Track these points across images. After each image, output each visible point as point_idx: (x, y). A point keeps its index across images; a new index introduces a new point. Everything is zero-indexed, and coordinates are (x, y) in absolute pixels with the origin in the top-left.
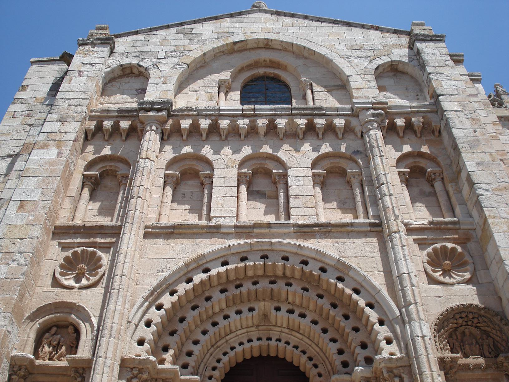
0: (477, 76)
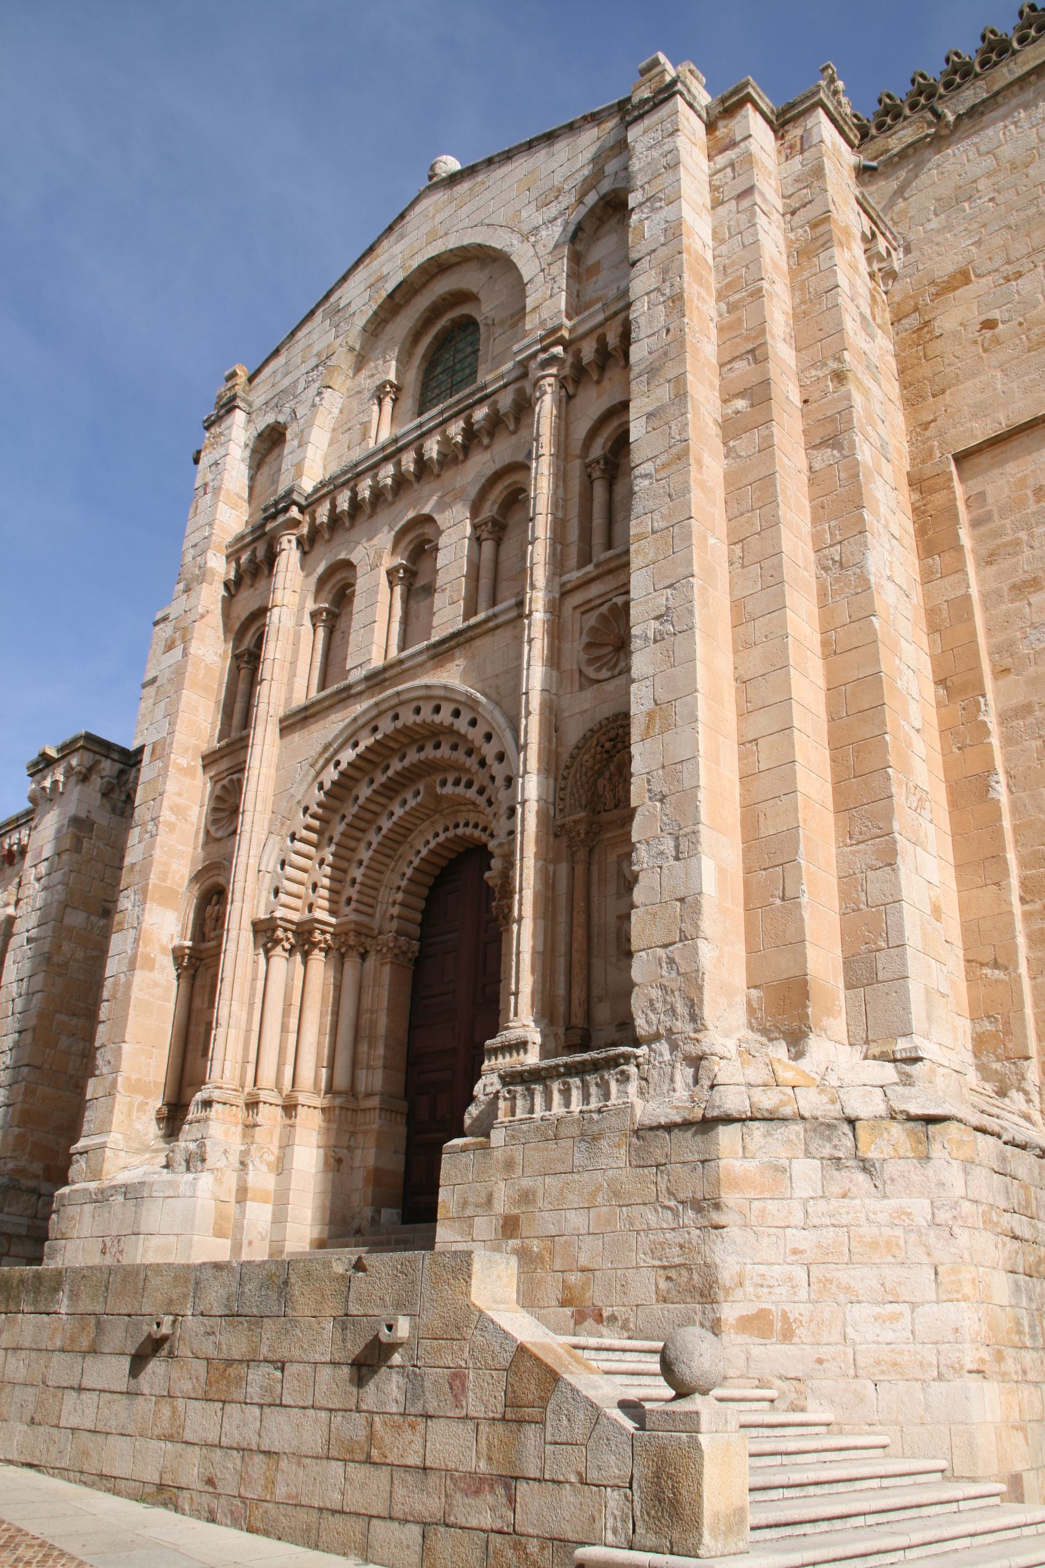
0: (808, 98)
